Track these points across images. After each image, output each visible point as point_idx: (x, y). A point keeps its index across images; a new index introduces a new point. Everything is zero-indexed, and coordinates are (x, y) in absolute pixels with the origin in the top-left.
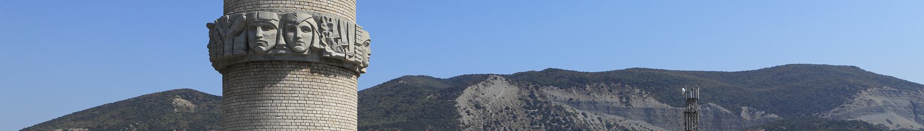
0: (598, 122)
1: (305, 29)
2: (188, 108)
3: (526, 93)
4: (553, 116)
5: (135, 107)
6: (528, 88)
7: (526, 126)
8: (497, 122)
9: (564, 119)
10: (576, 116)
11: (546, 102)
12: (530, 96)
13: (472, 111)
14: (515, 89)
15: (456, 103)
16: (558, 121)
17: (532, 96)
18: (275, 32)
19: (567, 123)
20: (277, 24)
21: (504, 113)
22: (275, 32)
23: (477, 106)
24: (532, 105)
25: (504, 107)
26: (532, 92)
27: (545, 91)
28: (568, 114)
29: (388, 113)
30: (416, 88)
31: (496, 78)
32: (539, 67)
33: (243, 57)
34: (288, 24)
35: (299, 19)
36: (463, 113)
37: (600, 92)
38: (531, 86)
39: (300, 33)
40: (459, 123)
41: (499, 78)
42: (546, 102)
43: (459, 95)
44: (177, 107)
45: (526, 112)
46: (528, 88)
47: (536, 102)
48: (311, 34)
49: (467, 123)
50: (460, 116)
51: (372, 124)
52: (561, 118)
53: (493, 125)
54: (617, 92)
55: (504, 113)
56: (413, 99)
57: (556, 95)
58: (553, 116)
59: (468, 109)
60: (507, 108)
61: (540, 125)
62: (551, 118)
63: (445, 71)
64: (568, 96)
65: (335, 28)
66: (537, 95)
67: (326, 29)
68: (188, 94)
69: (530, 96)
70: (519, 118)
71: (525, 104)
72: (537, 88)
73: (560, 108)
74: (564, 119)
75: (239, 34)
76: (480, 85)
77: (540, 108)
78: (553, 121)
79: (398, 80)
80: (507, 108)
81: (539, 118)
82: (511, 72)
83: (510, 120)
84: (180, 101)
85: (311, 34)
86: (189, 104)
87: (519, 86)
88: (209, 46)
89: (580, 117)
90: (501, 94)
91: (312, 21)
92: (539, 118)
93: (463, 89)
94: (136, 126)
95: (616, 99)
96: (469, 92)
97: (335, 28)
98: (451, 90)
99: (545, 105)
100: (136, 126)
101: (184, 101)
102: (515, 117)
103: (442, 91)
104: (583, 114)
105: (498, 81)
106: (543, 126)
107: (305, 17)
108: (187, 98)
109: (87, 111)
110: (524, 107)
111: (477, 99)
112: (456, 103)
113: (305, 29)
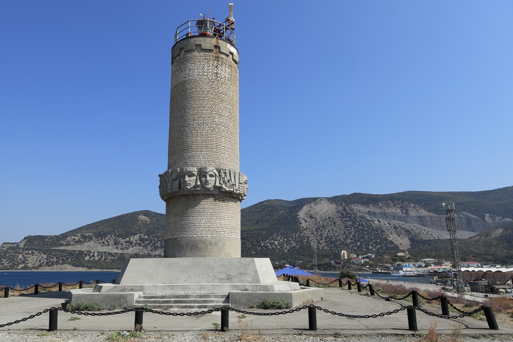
0: (388, 225)
1: (211, 176)
2: (146, 221)
3: (341, 208)
4: (358, 222)
5: (119, 221)
6: (342, 205)
7: (342, 228)
8: (323, 227)
9: (366, 224)
10: (373, 222)
11: (354, 214)
12: (343, 210)
13: (308, 220)
14: (334, 206)
15: (298, 215)
16: (362, 225)
17: (345, 210)
18: (195, 178)
19: (368, 226)
20: (196, 173)
21: (328, 221)
22: (195, 178)
23: (311, 217)
24: (345, 215)
25: (327, 217)
26: (344, 208)
27: (352, 207)
28: (368, 221)
29: (258, 222)
30: (274, 207)
31: (322, 200)
32: (348, 193)
33: (177, 192)
34: (202, 173)
35: (208, 170)
36: (303, 221)
37: (388, 207)
38: (344, 204)
39: (208, 178)
40: (300, 227)
41: (323, 199)
42: (354, 214)
43: (299, 210)
45: (342, 220)
46: (342, 205)
47: (347, 214)
48: (214, 178)
49: (305, 227)
50: (301, 223)
51: (248, 229)
52: (364, 223)
53: (321, 228)
54: (399, 206)
55: (328, 221)
56: (272, 213)
57: (359, 209)
58: (358, 222)
59: (306, 218)
60: (330, 218)
61: (351, 228)
63: (291, 196)
64: (367, 210)
65: (228, 174)
66: (348, 209)
67: (223, 175)
68: (146, 213)
69: (343, 210)
70: (337, 224)
71: (340, 215)
73: (363, 217)
74: (366, 224)
75: (175, 180)
76: (312, 204)
77: (351, 216)
78: (359, 225)
79: (263, 202)
80: (330, 218)
81: (350, 223)
84: (142, 217)
85: (214, 178)
86: (147, 219)
87: (336, 204)
88: (159, 187)
89: (376, 222)
90: (325, 209)
91: (215, 171)
92: (350, 223)
94: (118, 232)
95: (399, 211)
96: (305, 208)
97: (228, 174)
98: (295, 208)
99: (353, 215)
100: (118, 232)
101: (144, 217)
102: (334, 223)
103: (289, 208)
104: (378, 220)
105: (323, 202)
106: (353, 228)
107: (211, 169)
108: (146, 216)
110: (340, 217)
111: (311, 213)
112: (298, 215)
113: (211, 176)
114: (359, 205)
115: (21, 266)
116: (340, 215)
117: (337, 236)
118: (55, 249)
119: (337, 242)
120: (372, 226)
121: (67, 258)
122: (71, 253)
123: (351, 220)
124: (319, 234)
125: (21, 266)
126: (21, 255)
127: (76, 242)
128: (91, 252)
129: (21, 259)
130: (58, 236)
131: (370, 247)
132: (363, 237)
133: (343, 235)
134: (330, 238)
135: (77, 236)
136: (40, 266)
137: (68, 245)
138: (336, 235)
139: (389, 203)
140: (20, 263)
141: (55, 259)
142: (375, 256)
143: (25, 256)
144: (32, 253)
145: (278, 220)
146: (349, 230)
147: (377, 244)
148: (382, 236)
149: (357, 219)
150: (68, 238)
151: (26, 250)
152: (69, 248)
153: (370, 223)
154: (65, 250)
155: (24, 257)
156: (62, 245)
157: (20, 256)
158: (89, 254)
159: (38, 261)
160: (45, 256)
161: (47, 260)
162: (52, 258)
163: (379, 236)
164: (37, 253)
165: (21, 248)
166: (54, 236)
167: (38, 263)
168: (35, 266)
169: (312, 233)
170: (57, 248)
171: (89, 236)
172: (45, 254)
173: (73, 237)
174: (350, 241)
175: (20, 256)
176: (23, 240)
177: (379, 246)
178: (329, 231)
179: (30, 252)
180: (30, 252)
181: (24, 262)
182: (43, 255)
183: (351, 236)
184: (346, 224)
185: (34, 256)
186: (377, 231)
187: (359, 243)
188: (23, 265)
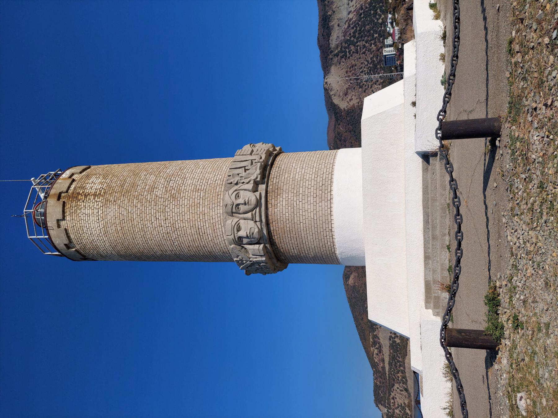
3: (336, 60)
4: (350, 38)
6: (332, 59)
7: (358, 57)
9: (353, 28)
10: (351, 19)
11: (341, 44)
12: (337, 56)
13: (349, 98)
14: (333, 69)
15: (344, 109)
16: (354, 33)
17: (337, 55)
19: (355, 26)
23: (346, 94)
24: (343, 54)
28: (349, 26)
30: (335, 137)
31: (326, 83)
38: (331, 56)
41: (326, 80)
42: (341, 44)
44: (355, 283)
45: (349, 58)
46: (332, 59)
47: (341, 51)
49: (358, 100)
52: (352, 31)
53: (359, 81)
56: (343, 138)
58: (350, 38)
59: (348, 100)
62: (352, 39)
66: (337, 51)
70: (353, 63)
71: (343, 60)
72: (332, 52)
76: (331, 93)
77: (346, 48)
78: (354, 37)
82: (322, 72)
83: (355, 69)
84: (351, 281)
86: (352, 276)
87: (331, 66)
93: (335, 105)
96: (336, 101)
98: (336, 114)
101: (351, 279)
103: (337, 120)
106: (358, 43)
109: (359, 333)
111: (341, 94)
112: (344, 109)
114: (331, 38)
115: (408, 411)
116: (343, 60)
117: (368, 62)
118: (389, 375)
119: (374, 61)
120: (356, 21)
121: (399, 361)
122: (393, 358)
123: (348, 47)
124: (365, 83)
125: (408, 411)
126: (396, 411)
127: (380, 351)
128: (391, 336)
129: (400, 411)
130: (374, 372)
131: (380, 21)
132: (369, 31)
133: (366, 55)
134: (370, 70)
135: (374, 351)
136: (406, 390)
137: (383, 361)
138: (366, 63)
139: (328, 2)
140: (405, 412)
141: (399, 375)
142: (390, 13)
143: (397, 406)
144: (393, 398)
145: (350, 132)
146: (360, 48)
147: (376, 13)
148: (366, 8)
149: (348, 40)
150: (376, 361)
151: (390, 405)
152: (387, 360)
153: (352, 24)
154: (389, 364)
155: (398, 407)
156: (383, 368)
157: (397, 411)
158: (393, 338)
159: (402, 392)
160: (396, 386)
161: (400, 383)
162: (398, 377)
163: (366, 12)
164: (393, 394)
165: (388, 411)
166: (374, 375)
167: (404, 393)
168: (407, 396)
169: (365, 92)
170: (387, 373)
171: (373, 338)
172: (394, 385)
173: (375, 356)
174: (373, 46)
175: (397, 411)
176: (379, 408)
177: (378, 10)
178: (362, 72)
179: (392, 401)
180: (392, 401)
181: (403, 408)
182: (395, 388)
183: (367, 45)
184: (353, 52)
185: (396, 396)
186: (361, 14)
187: (376, 35)
188: (407, 409)
